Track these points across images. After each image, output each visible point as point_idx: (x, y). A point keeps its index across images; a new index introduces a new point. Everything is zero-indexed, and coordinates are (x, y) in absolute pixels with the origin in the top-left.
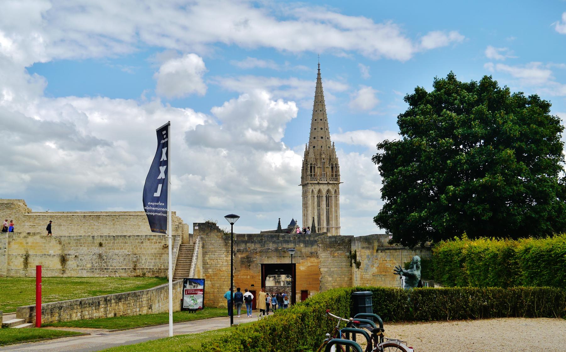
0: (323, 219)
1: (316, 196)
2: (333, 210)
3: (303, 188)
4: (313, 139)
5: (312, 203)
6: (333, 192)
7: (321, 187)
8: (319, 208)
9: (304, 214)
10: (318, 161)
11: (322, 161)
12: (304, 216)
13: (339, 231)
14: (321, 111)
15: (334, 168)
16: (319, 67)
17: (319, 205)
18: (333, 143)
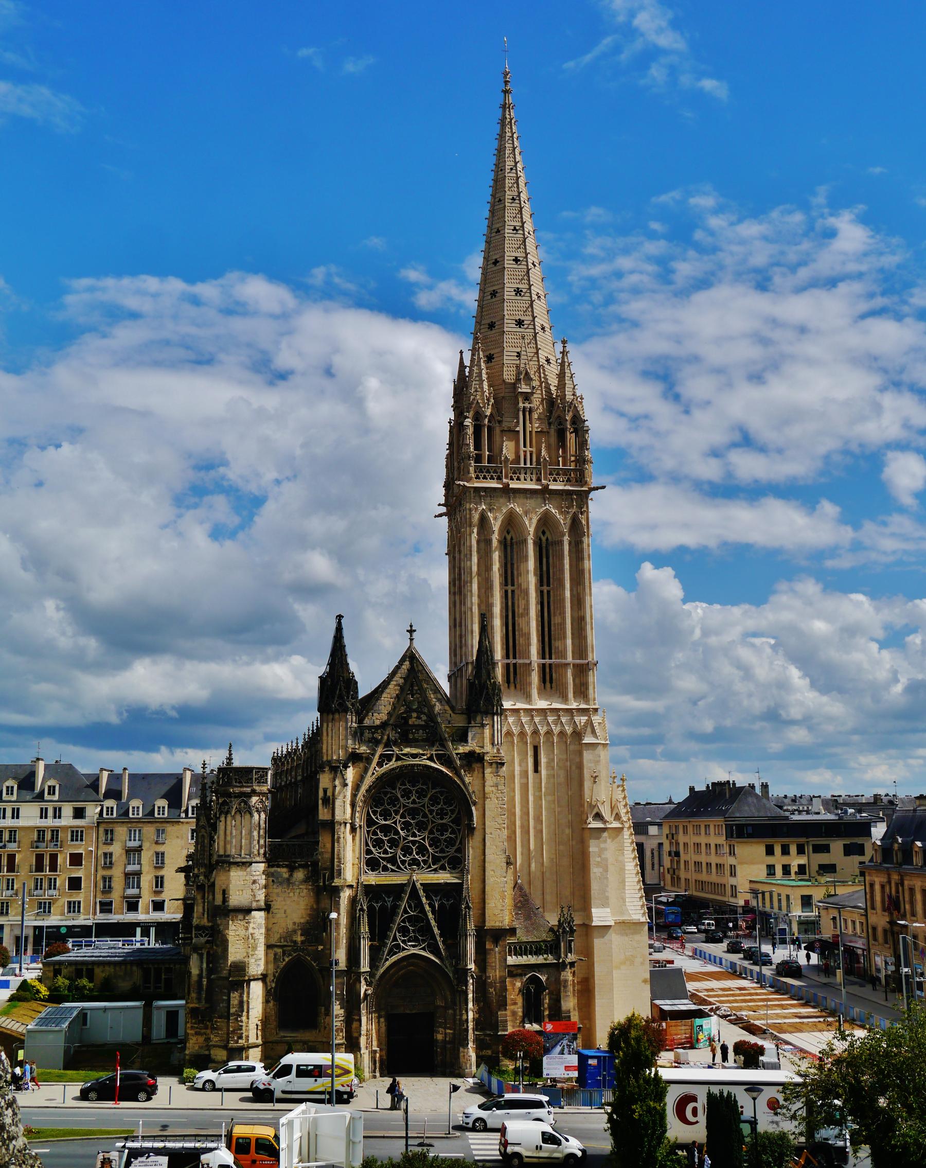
0: (525, 630)
1: (495, 538)
2: (568, 594)
3: (450, 521)
4: (485, 329)
5: (483, 568)
6: (563, 520)
8: (510, 588)
9: (455, 620)
10: (506, 405)
11: (521, 405)
12: (455, 626)
13: (591, 679)
14: (515, 229)
16: (506, 82)
17: (510, 575)
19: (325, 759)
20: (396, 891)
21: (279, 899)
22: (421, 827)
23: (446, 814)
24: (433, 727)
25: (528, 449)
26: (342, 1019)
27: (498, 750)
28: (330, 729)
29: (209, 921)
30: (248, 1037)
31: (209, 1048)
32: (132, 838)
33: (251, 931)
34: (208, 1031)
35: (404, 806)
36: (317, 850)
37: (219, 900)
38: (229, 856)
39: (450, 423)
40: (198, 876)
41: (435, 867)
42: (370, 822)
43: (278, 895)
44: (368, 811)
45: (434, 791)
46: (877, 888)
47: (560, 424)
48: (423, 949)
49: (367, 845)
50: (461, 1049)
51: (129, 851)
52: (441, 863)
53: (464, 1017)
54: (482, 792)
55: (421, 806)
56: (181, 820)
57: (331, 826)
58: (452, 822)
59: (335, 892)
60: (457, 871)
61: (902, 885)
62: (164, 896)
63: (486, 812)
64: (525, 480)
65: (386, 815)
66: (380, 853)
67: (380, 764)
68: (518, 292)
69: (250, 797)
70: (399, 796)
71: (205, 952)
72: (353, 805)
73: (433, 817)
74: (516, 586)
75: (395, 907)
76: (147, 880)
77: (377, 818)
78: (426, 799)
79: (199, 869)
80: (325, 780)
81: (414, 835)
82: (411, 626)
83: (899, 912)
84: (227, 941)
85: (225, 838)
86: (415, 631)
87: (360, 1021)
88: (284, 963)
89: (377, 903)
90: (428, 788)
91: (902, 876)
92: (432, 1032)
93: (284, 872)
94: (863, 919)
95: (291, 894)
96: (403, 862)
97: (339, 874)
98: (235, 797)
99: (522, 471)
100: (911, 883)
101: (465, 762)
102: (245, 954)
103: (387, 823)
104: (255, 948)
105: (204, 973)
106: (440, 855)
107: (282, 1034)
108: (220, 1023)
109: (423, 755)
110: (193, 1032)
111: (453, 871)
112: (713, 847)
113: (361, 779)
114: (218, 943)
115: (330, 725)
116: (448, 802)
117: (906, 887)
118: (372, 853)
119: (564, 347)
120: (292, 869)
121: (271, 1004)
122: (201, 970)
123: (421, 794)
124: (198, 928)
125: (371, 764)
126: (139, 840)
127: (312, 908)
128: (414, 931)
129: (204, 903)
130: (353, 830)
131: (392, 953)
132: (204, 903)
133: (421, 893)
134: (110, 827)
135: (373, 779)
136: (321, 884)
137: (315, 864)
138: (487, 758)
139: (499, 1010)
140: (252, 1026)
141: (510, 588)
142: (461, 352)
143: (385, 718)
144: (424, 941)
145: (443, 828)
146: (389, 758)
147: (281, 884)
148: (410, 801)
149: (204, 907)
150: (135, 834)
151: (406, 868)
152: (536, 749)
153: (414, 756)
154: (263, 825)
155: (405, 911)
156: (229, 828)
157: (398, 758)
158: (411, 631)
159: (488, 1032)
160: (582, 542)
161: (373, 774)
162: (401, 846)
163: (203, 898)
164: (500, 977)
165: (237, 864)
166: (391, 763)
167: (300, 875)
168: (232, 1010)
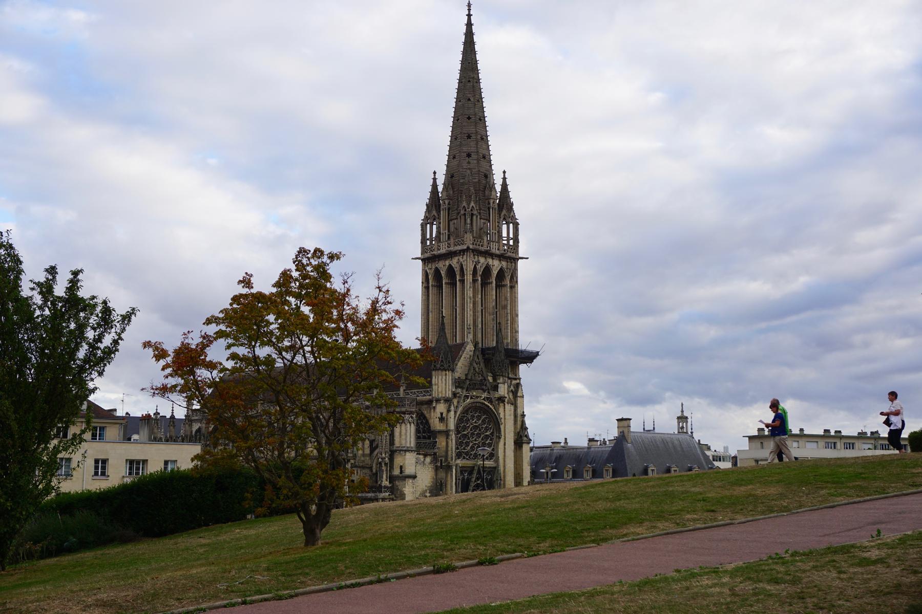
16: (469, 10)
20: (471, 470)
21: (420, 472)
22: (479, 435)
23: (488, 430)
25: (494, 232)
29: (390, 483)
36: (435, 446)
38: (404, 447)
40: (385, 458)
43: (419, 471)
55: (479, 425)
57: (447, 433)
58: (490, 434)
59: (449, 468)
60: (492, 460)
63: (506, 430)
65: (465, 428)
69: (413, 414)
79: (385, 454)
80: (441, 408)
81: (475, 440)
84: (405, 494)
85: (400, 437)
93: (421, 457)
95: (425, 470)
98: (408, 414)
99: (492, 243)
101: (497, 402)
103: (465, 433)
109: (481, 397)
114: (397, 495)
116: (489, 423)
119: (504, 175)
120: (425, 455)
123: (479, 418)
124: (385, 487)
129: (387, 474)
132: (387, 474)
136: (439, 465)
137: (435, 454)
138: (506, 401)
146: (467, 397)
147: (420, 464)
148: (474, 421)
149: (387, 476)
153: (477, 397)
155: (475, 481)
156: (403, 431)
157: (471, 398)
160: (514, 287)
162: (470, 445)
163: (387, 470)
165: (409, 451)
166: (469, 400)
167: (428, 459)
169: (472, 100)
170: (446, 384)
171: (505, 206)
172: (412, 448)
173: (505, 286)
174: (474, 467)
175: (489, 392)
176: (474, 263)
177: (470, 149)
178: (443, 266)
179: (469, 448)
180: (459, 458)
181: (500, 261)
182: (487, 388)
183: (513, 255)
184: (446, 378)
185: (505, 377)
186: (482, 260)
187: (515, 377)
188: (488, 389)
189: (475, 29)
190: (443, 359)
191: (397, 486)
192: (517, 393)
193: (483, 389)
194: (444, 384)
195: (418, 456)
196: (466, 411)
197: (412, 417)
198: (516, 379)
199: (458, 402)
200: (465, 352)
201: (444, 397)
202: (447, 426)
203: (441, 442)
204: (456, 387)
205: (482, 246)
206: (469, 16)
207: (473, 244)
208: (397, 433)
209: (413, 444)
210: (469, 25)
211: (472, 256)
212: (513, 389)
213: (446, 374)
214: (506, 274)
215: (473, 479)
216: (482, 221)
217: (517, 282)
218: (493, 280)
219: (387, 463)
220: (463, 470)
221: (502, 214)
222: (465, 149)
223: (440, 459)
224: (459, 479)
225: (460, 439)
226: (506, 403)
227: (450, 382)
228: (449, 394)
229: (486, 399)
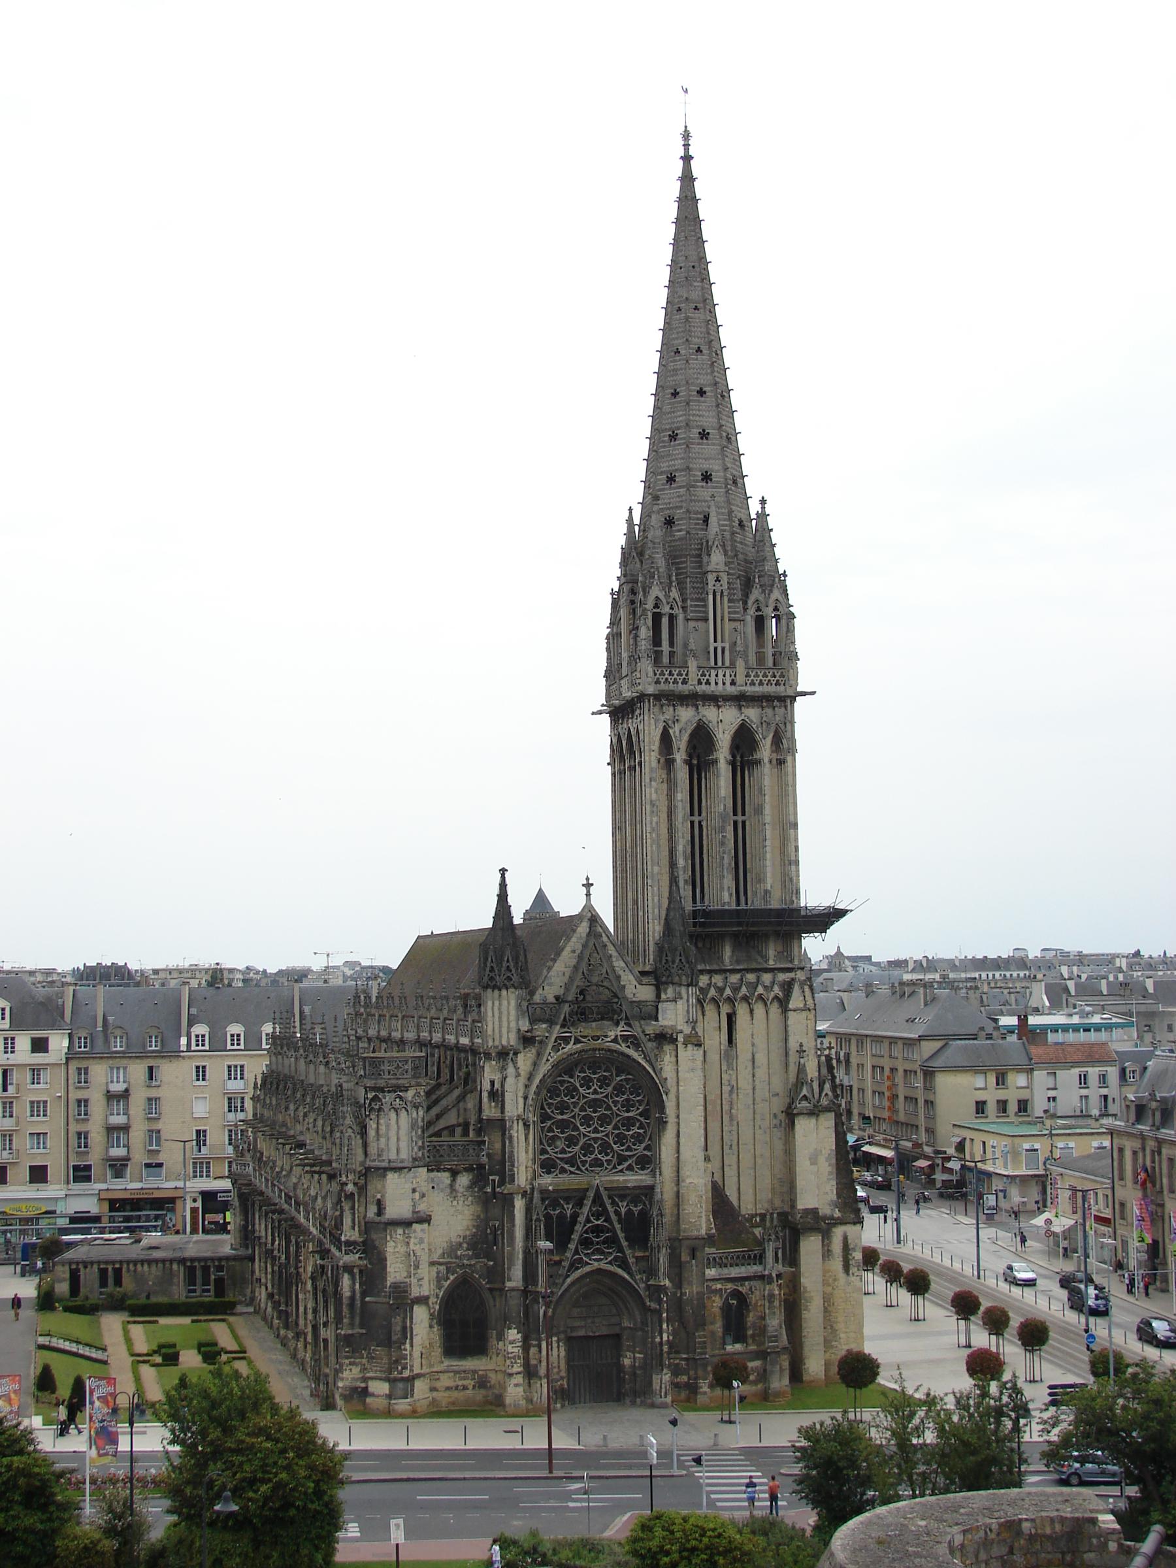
7: (710, 713)
8: (696, 819)
15: (768, 623)
18: (763, 501)
19: (490, 1044)
20: (578, 1197)
22: (604, 1120)
24: (617, 1003)
26: (520, 1344)
27: (693, 1028)
28: (496, 1009)
30: (412, 1366)
31: (365, 1380)
32: (115, 1080)
33: (412, 1246)
34: (364, 1361)
35: (584, 1097)
37: (372, 1211)
38: (384, 1160)
39: (612, 594)
40: (347, 1184)
41: (620, 1168)
42: (544, 1117)
44: (542, 1104)
45: (619, 1079)
46: (1128, 1154)
47: (758, 609)
48: (610, 1263)
49: (541, 1143)
50: (654, 1376)
51: (110, 1097)
52: (626, 1164)
53: (658, 1340)
54: (675, 1079)
55: (606, 1097)
56: (182, 1054)
57: (501, 1125)
58: (641, 1115)
59: (508, 1201)
60: (646, 1172)
61: (1160, 1153)
62: (161, 1158)
64: (716, 684)
65: (563, 1107)
66: (556, 1153)
67: (556, 1048)
68: (704, 435)
69: (407, 1091)
70: (578, 1085)
71: (356, 1270)
72: (526, 1098)
73: (618, 1109)
74: (704, 814)
75: (575, 1216)
76: (138, 1134)
77: (552, 1112)
78: (610, 1089)
79: (347, 1176)
81: (596, 1131)
82: (588, 879)
83: (1154, 1186)
86: (592, 885)
87: (540, 1347)
88: (448, 1282)
89: (554, 1210)
90: (611, 1075)
91: (1159, 1142)
92: (619, 1356)
93: (445, 1177)
94: (1109, 1192)
96: (584, 1163)
97: (512, 1180)
98: (389, 1092)
99: (713, 673)
100: (1171, 1152)
101: (654, 1044)
102: (406, 1274)
103: (564, 1117)
104: (417, 1267)
105: (358, 1296)
106: (627, 1153)
107: (447, 1362)
108: (379, 1351)
110: (347, 1361)
111: (642, 1172)
112: (901, 1072)
113: (535, 1064)
115: (497, 1003)
116: (636, 1090)
117: (1164, 1157)
118: (548, 1153)
119: (763, 508)
120: (454, 1174)
121: (435, 1329)
122: (353, 1292)
123: (604, 1082)
124: (348, 1243)
125: (546, 1049)
126: (124, 1082)
127: (478, 1217)
128: (598, 1243)
129: (354, 1214)
130: (526, 1126)
131: (573, 1267)
132: (354, 1214)
133: (605, 1198)
134: (83, 1064)
135: (548, 1066)
138: (681, 1038)
139: (697, 1331)
140: (416, 1354)
141: (696, 819)
142: (630, 509)
143: (561, 992)
144: (611, 1253)
145: (629, 1123)
146: (566, 1040)
148: (591, 1091)
149: (353, 1220)
150: (118, 1073)
151: (587, 1169)
152: (731, 1019)
154: (420, 1124)
155: (588, 1221)
156: (383, 1128)
157: (577, 1041)
158: (588, 885)
159: (684, 1356)
161: (548, 1060)
162: (581, 1144)
163: (353, 1208)
164: (697, 1293)
166: (569, 1047)
167: (464, 1180)
168: (394, 1338)
169: (683, 352)
170: (500, 1018)
171: (757, 580)
172: (402, 1161)
173: (758, 762)
174: (587, 1190)
175: (629, 1025)
176: (661, 726)
177: (674, 465)
178: (623, 729)
179: (578, 1148)
180: (549, 1172)
181: (740, 709)
182: (623, 1015)
183: (780, 690)
184: (500, 1004)
185: (681, 985)
186: (686, 714)
187: (790, 965)
188: (627, 1018)
189: (700, 189)
190: (494, 965)
191: (373, 1241)
192: (788, 1001)
193: (611, 1019)
194: (496, 1019)
195: (435, 1174)
196: (566, 1068)
197: (401, 1098)
198: (790, 970)
199: (539, 1055)
200: (574, 939)
201: (496, 1047)
202: (503, 1112)
203: (493, 1142)
204: (532, 1022)
205: (685, 682)
206: (687, 159)
207: (658, 682)
208: (372, 1133)
209: (404, 1155)
210: (687, 179)
211: (656, 709)
212: (781, 995)
213: (500, 996)
214: (759, 737)
215: (582, 1219)
216: (692, 624)
217: (792, 750)
218: (723, 753)
219: (352, 1194)
220: (551, 1198)
221: (750, 602)
222: (664, 466)
223: (491, 1178)
224: (538, 1220)
225: (550, 1130)
226: (681, 1046)
227: (513, 1012)
228: (512, 1040)
229: (620, 1041)
